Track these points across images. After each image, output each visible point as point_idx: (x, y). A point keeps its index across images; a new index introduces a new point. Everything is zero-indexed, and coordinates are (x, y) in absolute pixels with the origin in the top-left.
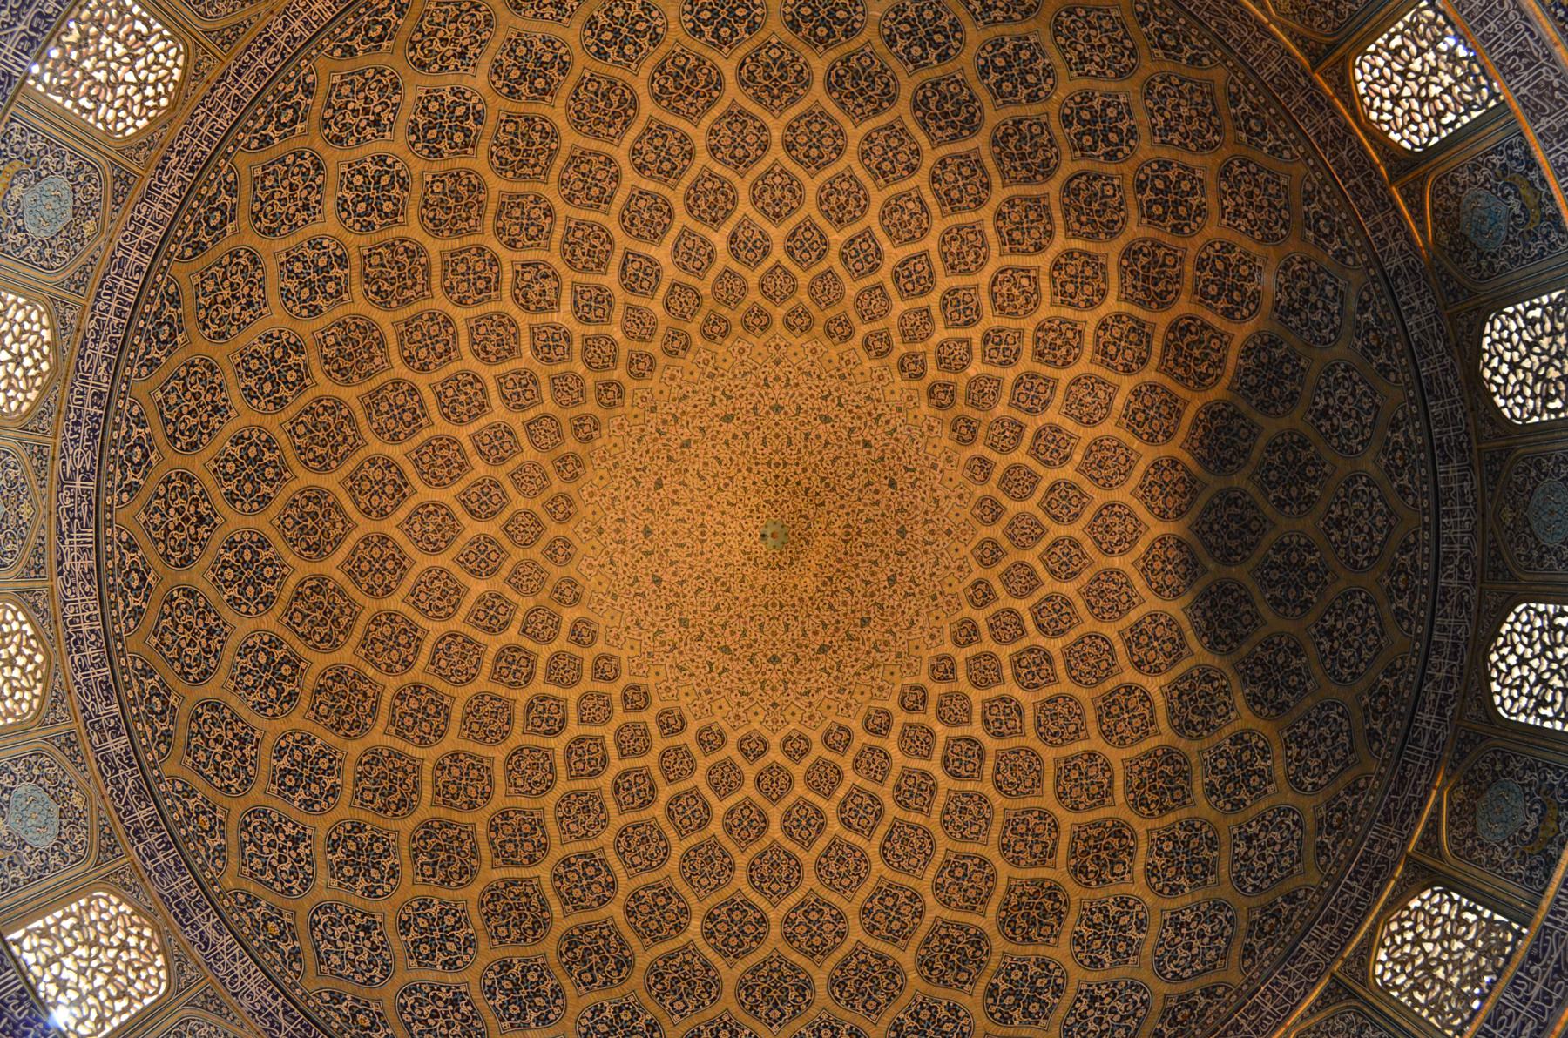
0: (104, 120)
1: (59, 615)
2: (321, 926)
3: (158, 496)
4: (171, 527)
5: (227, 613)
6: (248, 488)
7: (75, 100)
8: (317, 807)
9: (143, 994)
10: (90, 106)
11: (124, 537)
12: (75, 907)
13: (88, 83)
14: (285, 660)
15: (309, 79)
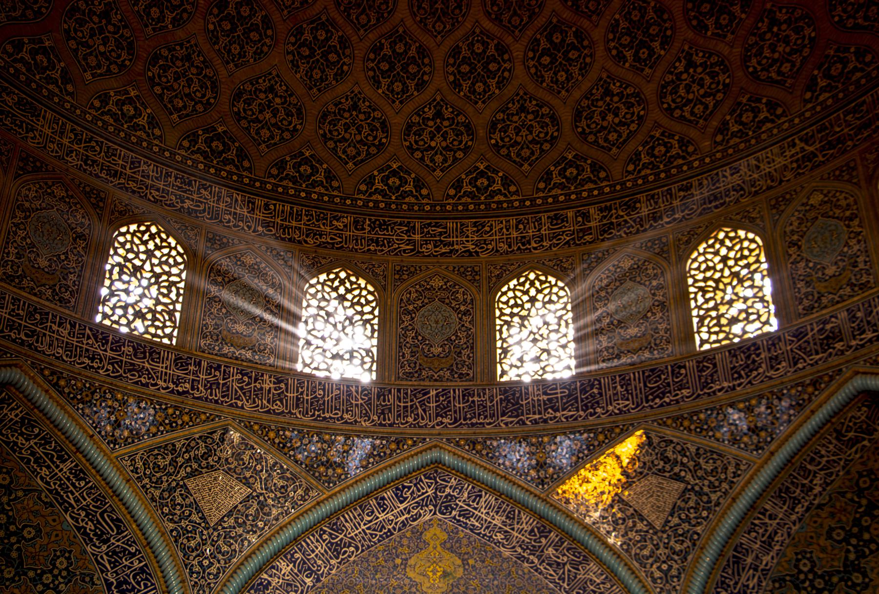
0: (179, 275)
1: (505, 257)
2: (759, 68)
3: (422, 159)
4: (444, 144)
5: (510, 90)
6: (412, 69)
7: (174, 303)
8: (669, 33)
9: (757, 261)
10: (174, 289)
11: (452, 192)
12: (692, 289)
13: (160, 297)
14: (549, 39)
15: (97, 104)
